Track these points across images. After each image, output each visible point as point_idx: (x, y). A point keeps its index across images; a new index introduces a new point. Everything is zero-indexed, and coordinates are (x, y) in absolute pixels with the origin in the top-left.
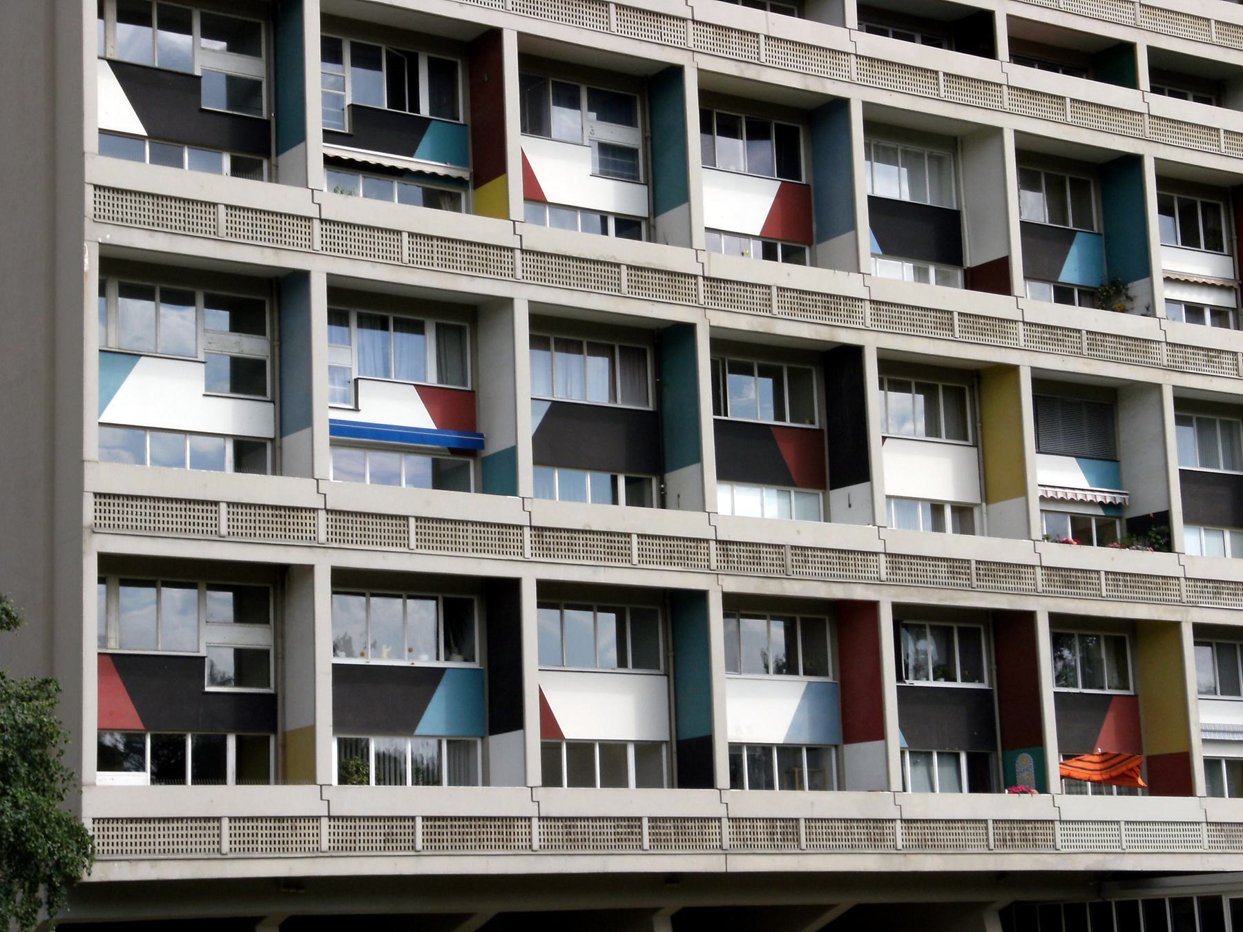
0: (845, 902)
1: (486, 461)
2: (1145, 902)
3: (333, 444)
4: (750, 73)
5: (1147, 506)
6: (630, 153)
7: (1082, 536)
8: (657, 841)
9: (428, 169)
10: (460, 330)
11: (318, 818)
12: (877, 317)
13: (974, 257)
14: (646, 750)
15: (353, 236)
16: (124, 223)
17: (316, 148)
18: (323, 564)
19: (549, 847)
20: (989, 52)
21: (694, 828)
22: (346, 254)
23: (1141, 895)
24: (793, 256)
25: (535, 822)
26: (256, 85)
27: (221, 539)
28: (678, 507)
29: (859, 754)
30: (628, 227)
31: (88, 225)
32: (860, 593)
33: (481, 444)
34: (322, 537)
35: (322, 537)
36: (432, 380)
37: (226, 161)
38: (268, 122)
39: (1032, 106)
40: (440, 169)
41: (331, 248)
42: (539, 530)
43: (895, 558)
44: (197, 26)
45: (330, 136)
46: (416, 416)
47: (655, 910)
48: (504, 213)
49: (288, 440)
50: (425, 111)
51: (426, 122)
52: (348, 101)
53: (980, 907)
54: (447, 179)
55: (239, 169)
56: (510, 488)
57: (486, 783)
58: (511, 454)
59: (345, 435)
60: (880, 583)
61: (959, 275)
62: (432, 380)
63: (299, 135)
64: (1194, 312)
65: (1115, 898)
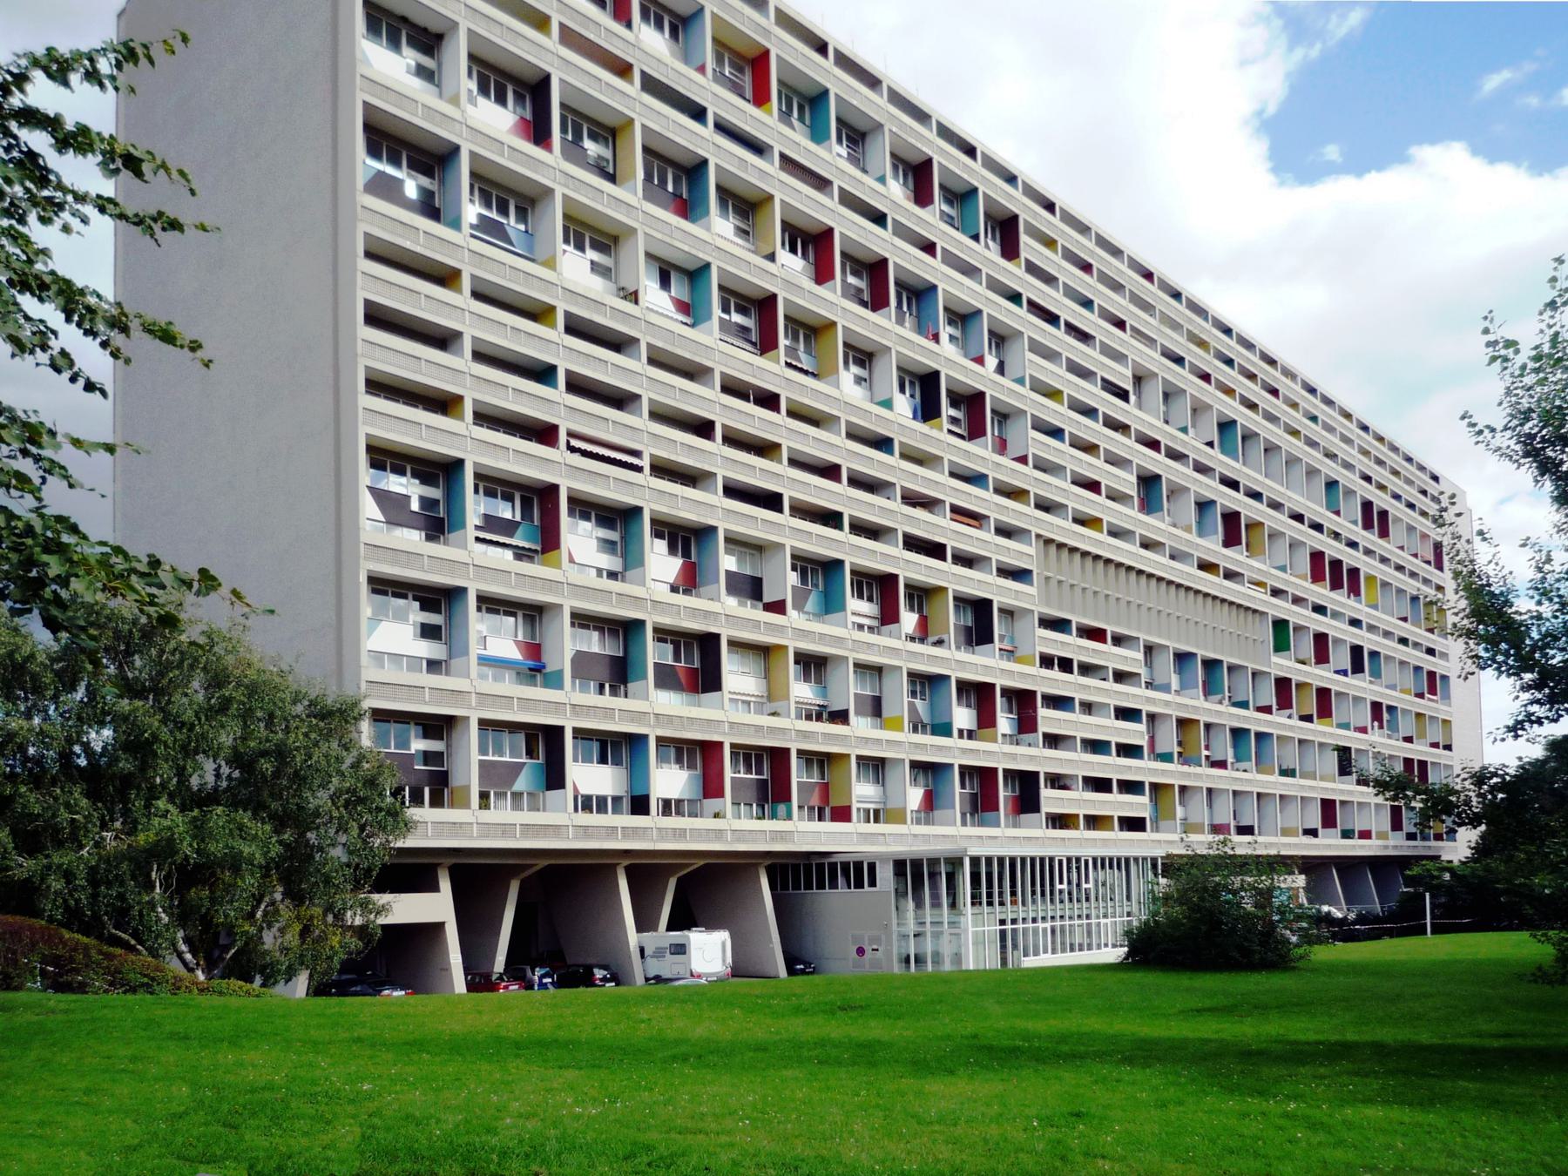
1: (545, 674)
2: (829, 863)
3: (479, 664)
5: (836, 706)
6: (613, 543)
7: (809, 717)
8: (624, 836)
9: (521, 545)
11: (472, 824)
12: (727, 621)
13: (767, 598)
14: (616, 800)
16: (378, 561)
17: (471, 533)
19: (576, 838)
20: (780, 511)
23: (826, 861)
24: (687, 592)
25: (570, 828)
26: (437, 502)
27: (426, 703)
28: (634, 698)
29: (712, 804)
30: (613, 575)
31: (362, 561)
32: (716, 738)
33: (544, 667)
34: (474, 705)
35: (474, 705)
38: (443, 519)
40: (527, 545)
43: (731, 724)
44: (409, 473)
45: (477, 528)
46: (514, 654)
47: (618, 864)
48: (559, 567)
49: (453, 661)
50: (518, 518)
52: (482, 512)
53: (756, 866)
54: (530, 550)
55: (429, 538)
56: (560, 686)
57: (544, 810)
58: (560, 673)
59: (485, 661)
60: (724, 733)
61: (761, 605)
62: (520, 638)
63: (462, 525)
64: (861, 627)
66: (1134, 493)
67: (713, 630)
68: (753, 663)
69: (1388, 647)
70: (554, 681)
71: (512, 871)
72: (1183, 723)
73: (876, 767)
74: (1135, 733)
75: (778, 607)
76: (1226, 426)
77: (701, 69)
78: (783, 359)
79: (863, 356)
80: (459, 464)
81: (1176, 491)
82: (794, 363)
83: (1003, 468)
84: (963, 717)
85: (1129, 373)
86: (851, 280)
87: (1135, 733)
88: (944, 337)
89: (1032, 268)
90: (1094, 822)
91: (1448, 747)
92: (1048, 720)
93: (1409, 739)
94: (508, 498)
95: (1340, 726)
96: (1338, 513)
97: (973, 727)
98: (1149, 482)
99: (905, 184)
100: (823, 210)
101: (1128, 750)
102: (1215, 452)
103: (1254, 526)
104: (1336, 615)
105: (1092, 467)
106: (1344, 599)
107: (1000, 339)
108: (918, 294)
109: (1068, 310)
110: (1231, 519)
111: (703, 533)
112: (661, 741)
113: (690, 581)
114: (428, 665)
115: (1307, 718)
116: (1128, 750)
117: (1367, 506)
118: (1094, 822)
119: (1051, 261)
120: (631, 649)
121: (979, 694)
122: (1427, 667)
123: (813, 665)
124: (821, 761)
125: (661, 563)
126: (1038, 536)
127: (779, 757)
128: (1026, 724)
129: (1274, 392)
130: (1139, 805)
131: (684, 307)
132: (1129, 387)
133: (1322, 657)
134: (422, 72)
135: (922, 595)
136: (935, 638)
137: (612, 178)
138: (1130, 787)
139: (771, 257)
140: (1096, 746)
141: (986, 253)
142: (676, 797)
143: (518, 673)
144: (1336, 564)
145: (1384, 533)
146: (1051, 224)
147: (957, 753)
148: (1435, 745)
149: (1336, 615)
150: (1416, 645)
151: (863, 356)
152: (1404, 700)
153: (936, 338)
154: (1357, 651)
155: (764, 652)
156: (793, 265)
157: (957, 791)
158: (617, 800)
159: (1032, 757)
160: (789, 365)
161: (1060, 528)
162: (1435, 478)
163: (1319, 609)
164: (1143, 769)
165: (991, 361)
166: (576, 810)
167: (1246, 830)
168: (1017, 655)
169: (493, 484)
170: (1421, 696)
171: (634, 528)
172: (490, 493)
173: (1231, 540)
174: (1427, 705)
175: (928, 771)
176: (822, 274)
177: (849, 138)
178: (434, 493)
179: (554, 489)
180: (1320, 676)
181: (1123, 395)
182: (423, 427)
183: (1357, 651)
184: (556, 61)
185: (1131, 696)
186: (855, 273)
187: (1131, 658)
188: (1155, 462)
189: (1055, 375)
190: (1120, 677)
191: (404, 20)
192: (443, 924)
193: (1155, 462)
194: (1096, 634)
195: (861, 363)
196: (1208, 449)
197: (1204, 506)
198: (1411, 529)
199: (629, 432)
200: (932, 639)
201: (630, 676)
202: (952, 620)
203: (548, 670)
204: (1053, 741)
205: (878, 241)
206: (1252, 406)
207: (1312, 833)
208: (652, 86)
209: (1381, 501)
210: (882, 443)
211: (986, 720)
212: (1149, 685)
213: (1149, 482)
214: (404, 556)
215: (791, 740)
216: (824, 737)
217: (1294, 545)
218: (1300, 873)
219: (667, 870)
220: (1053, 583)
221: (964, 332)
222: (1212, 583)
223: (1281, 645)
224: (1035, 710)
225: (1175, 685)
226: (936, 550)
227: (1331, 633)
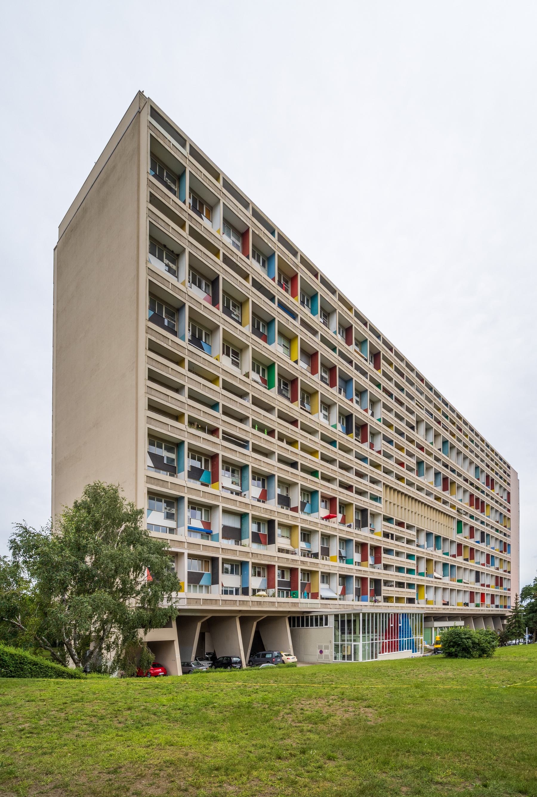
0: (266, 615)
3: (188, 530)
4: (260, 468)
10: (208, 511)
13: (292, 505)
15: (193, 491)
16: (151, 484)
18: (186, 552)
21: (245, 602)
22: (191, 494)
24: (264, 502)
30: (238, 494)
32: (273, 563)
33: (212, 532)
36: (203, 520)
37: (168, 473)
38: (176, 467)
39: (304, 480)
41: (188, 493)
42: (222, 549)
50: (203, 468)
51: (203, 470)
55: (170, 475)
65: (305, 615)
66: (415, 468)
67: (273, 518)
68: (286, 533)
69: (493, 532)
70: (215, 538)
71: (199, 618)
72: (428, 561)
73: (326, 577)
74: (411, 564)
75: (295, 510)
76: (445, 442)
77: (274, 279)
78: (300, 406)
79: (327, 406)
80: (183, 442)
81: (429, 468)
82: (303, 408)
83: (372, 456)
84: (357, 557)
85: (415, 420)
86: (323, 374)
87: (411, 564)
88: (354, 401)
89: (385, 374)
90: (399, 600)
91: (509, 572)
92: (386, 558)
93: (498, 569)
94: (200, 460)
95: (476, 563)
96: (478, 479)
97: (360, 561)
98: (420, 463)
99: (342, 336)
100: (315, 343)
101: (410, 571)
102: (441, 453)
103: (453, 483)
104: (477, 519)
105: (402, 456)
106: (479, 513)
107: (374, 402)
108: (347, 381)
109: (396, 392)
110: (445, 479)
111: (270, 477)
112: (255, 565)
113: (264, 497)
114: (169, 531)
115: (466, 560)
116: (410, 571)
117: (488, 476)
118: (399, 600)
119: (391, 371)
120: (243, 526)
121: (362, 547)
122: (504, 541)
123: (307, 535)
124: (308, 574)
125: (255, 490)
126: (384, 484)
127: (293, 571)
128: (378, 560)
129: (460, 430)
130: (412, 593)
131: (264, 381)
132: (415, 425)
133: (472, 536)
134: (170, 270)
135: (345, 506)
136: (349, 524)
137: (240, 324)
138: (410, 586)
139: (296, 362)
140: (399, 569)
141: (369, 366)
142: (258, 588)
143: (202, 535)
144: (477, 499)
145: (492, 488)
146: (391, 356)
147: (355, 571)
148: (505, 571)
149: (477, 519)
150: (501, 532)
151: (327, 406)
152: (496, 553)
153: (351, 400)
154: (482, 533)
155: (291, 528)
156: (303, 366)
157: (354, 585)
158: (237, 590)
159: (379, 573)
160: (301, 408)
161: (391, 480)
162: (509, 467)
163: (472, 517)
164: (414, 578)
165: (370, 412)
166: (222, 594)
167: (447, 604)
168: (375, 532)
169: (195, 453)
170: (501, 552)
171: (245, 475)
172: (193, 458)
173: (445, 489)
174: (504, 556)
175: (345, 579)
176: (314, 371)
177: (324, 315)
178: (173, 456)
179: (217, 455)
180: (471, 543)
181: (412, 428)
182: (169, 426)
183: (482, 533)
184: (221, 270)
185: (413, 549)
186: (325, 372)
187: (411, 534)
188: (422, 455)
189: (391, 418)
190: (409, 542)
191: (165, 246)
192: (173, 641)
193: (422, 455)
194: (400, 524)
195: (326, 409)
196: (439, 451)
197: (437, 474)
198: (501, 486)
199: (244, 433)
200: (347, 525)
201: (243, 537)
202: (353, 516)
203: (214, 533)
204: (386, 567)
205: (334, 358)
206: (453, 435)
207: (466, 604)
208: (256, 285)
209: (492, 475)
210: (333, 443)
211: (364, 559)
212: (418, 546)
213: (420, 463)
214: (161, 482)
215: (299, 565)
216: (310, 563)
217: (465, 491)
218: (462, 620)
219: (253, 618)
220: (388, 503)
221: (361, 399)
222: (438, 505)
223: (459, 531)
224: (381, 555)
225: (426, 546)
226: (349, 488)
227: (475, 526)
